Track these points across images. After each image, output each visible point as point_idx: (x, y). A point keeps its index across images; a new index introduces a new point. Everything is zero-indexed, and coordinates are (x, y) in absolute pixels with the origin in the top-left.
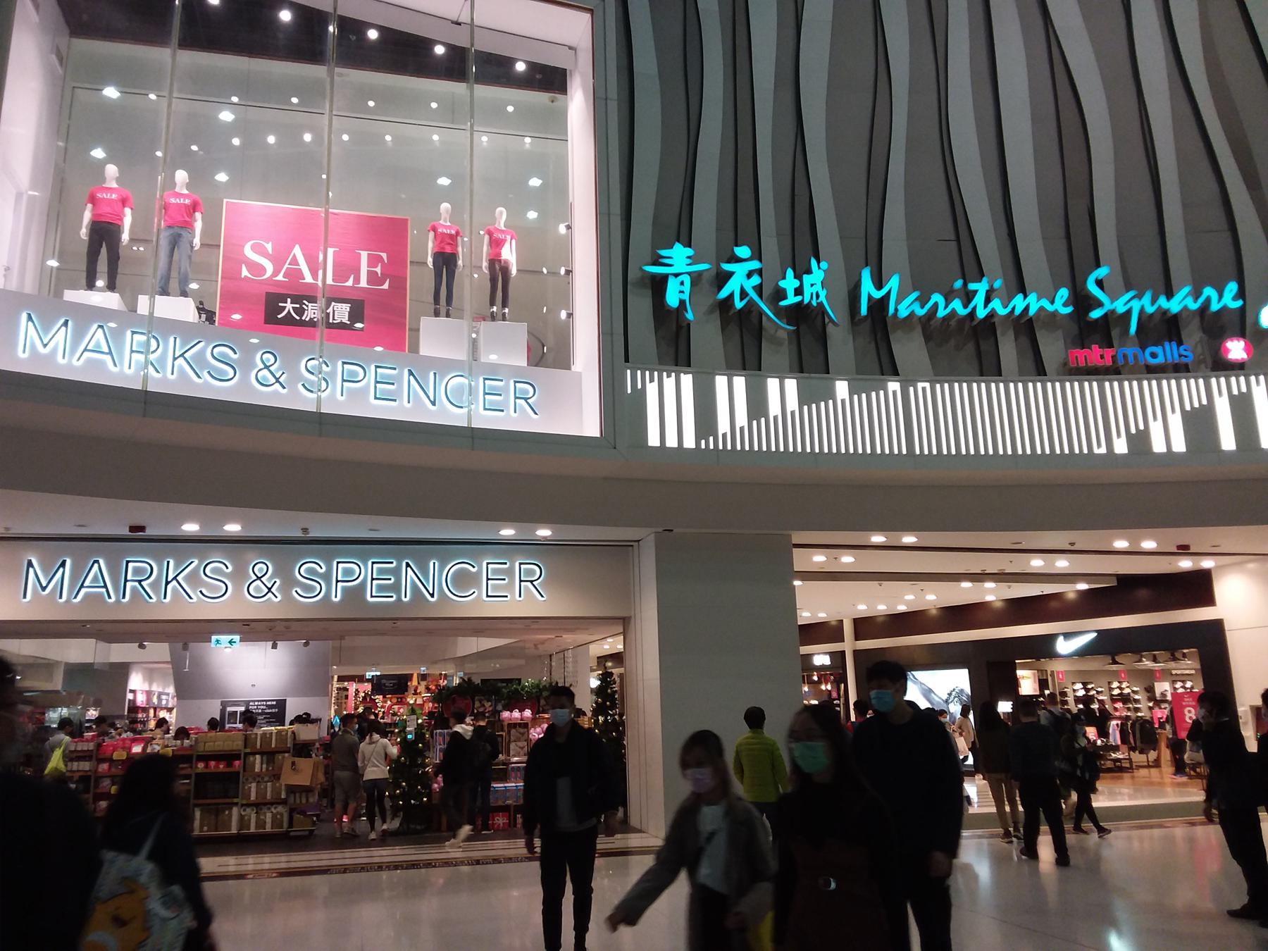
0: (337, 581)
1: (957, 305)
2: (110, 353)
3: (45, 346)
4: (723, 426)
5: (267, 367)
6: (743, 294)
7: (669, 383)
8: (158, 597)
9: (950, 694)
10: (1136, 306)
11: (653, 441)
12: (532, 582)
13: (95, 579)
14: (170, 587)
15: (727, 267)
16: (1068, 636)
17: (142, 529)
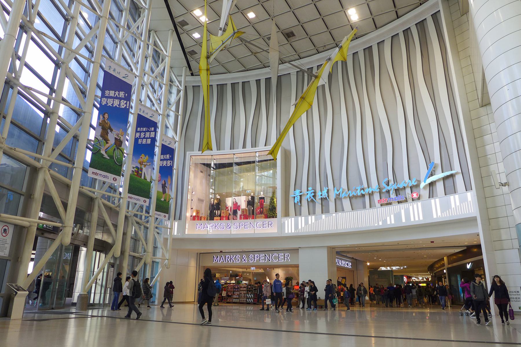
4: (300, 227)
11: (286, 232)
17: (222, 251)
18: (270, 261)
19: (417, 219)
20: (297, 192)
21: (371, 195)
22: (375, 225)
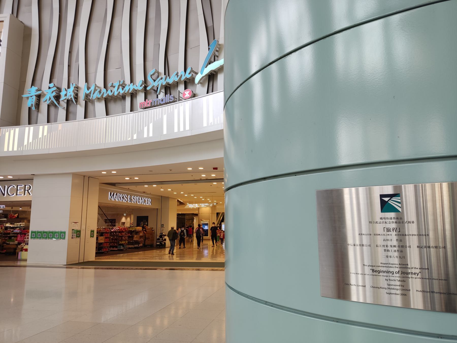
4: (26, 143)
11: (6, 149)
18: (4, 195)
19: (182, 129)
20: (34, 88)
21: (133, 95)
22: (128, 139)
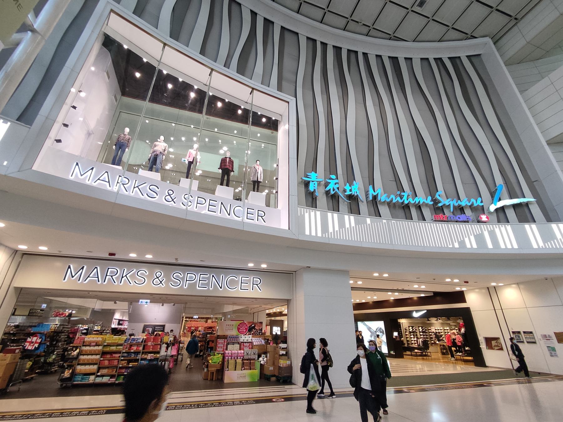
0: (186, 281)
1: (398, 199)
2: (109, 182)
3: (82, 175)
4: (331, 230)
5: (169, 195)
6: (334, 190)
7: (313, 214)
8: (118, 283)
9: (377, 329)
10: (452, 203)
11: (307, 233)
12: (257, 285)
13: (94, 274)
14: (123, 279)
15: (329, 181)
16: (417, 311)
17: (114, 255)
